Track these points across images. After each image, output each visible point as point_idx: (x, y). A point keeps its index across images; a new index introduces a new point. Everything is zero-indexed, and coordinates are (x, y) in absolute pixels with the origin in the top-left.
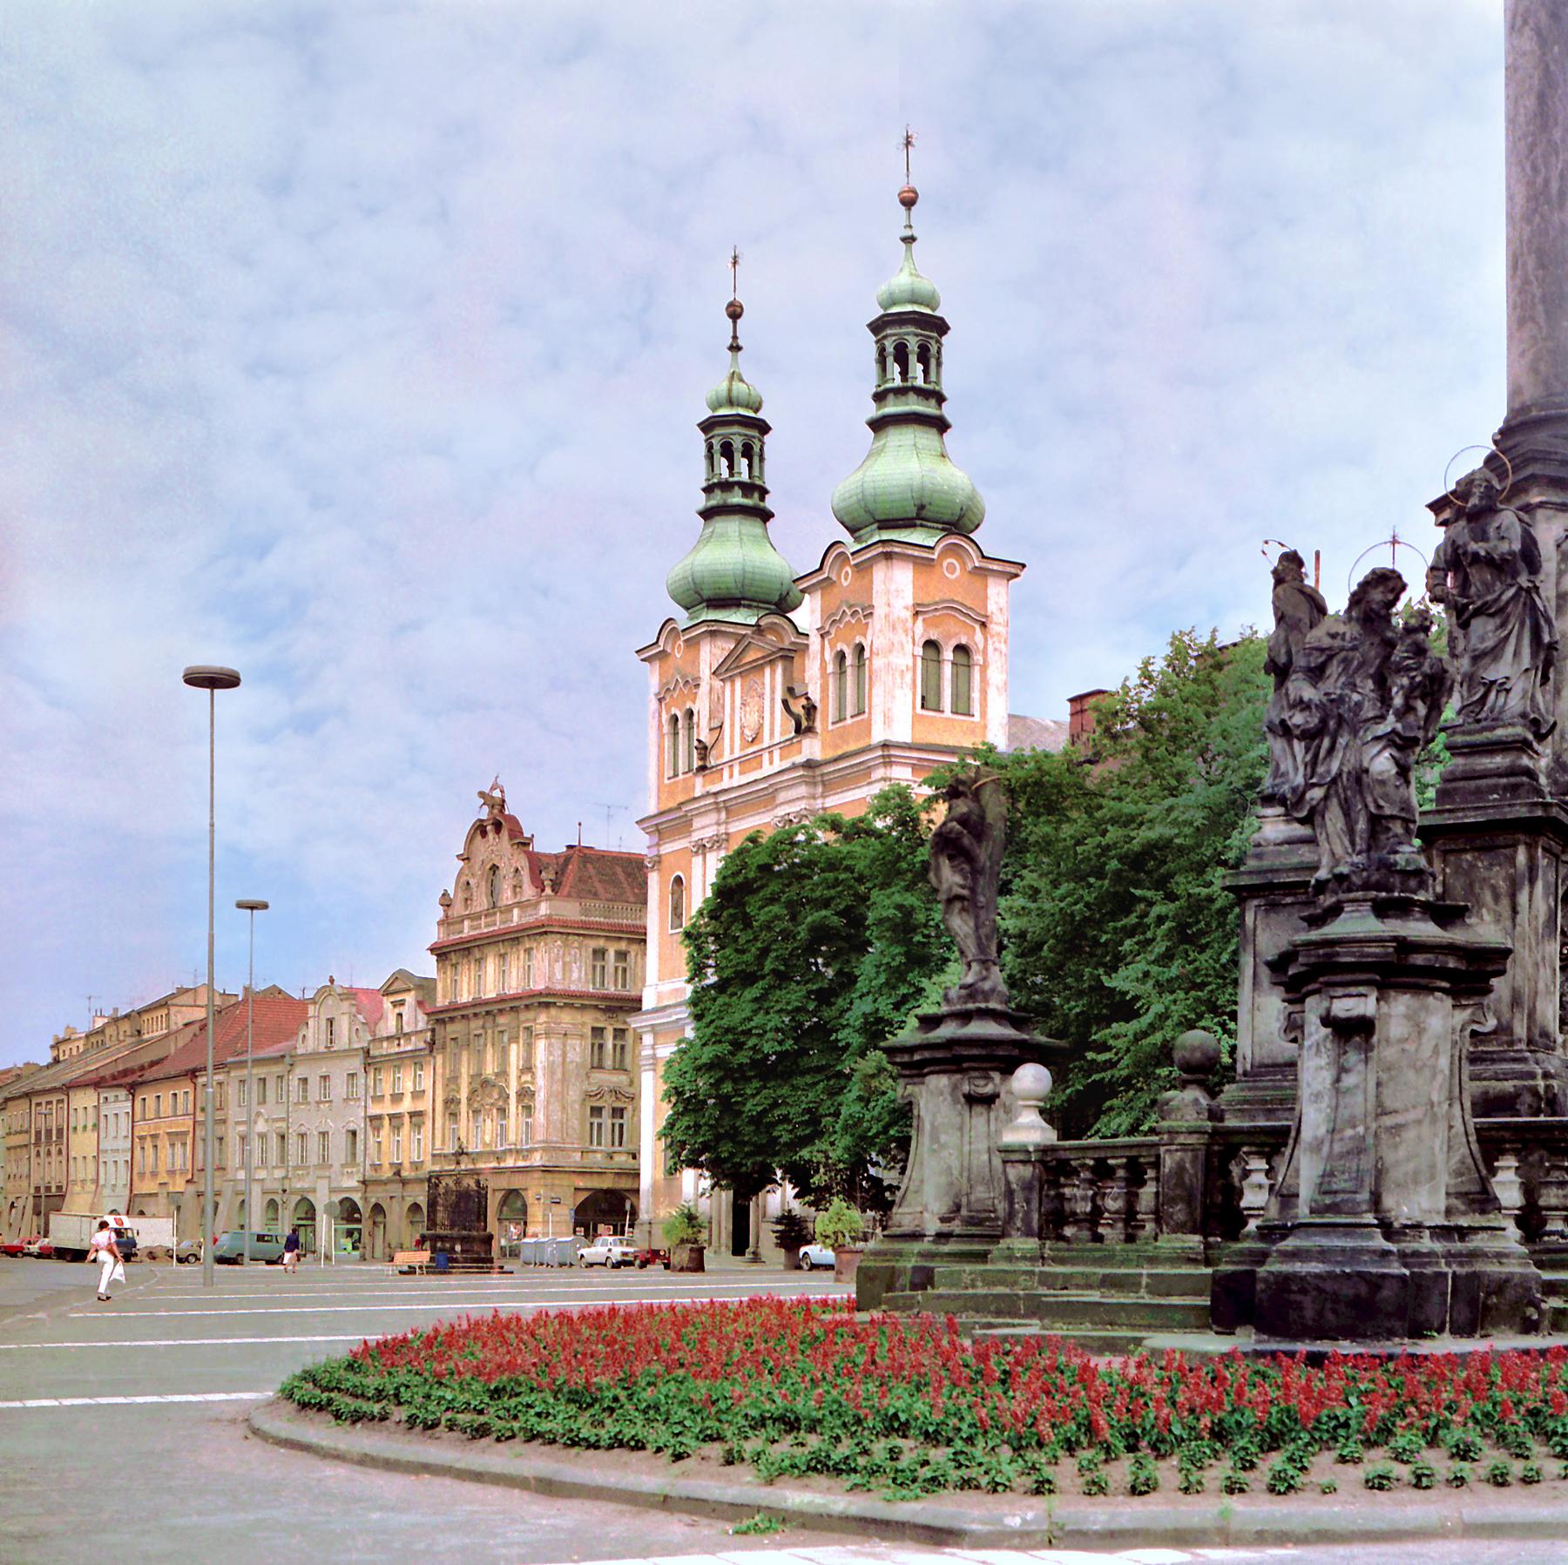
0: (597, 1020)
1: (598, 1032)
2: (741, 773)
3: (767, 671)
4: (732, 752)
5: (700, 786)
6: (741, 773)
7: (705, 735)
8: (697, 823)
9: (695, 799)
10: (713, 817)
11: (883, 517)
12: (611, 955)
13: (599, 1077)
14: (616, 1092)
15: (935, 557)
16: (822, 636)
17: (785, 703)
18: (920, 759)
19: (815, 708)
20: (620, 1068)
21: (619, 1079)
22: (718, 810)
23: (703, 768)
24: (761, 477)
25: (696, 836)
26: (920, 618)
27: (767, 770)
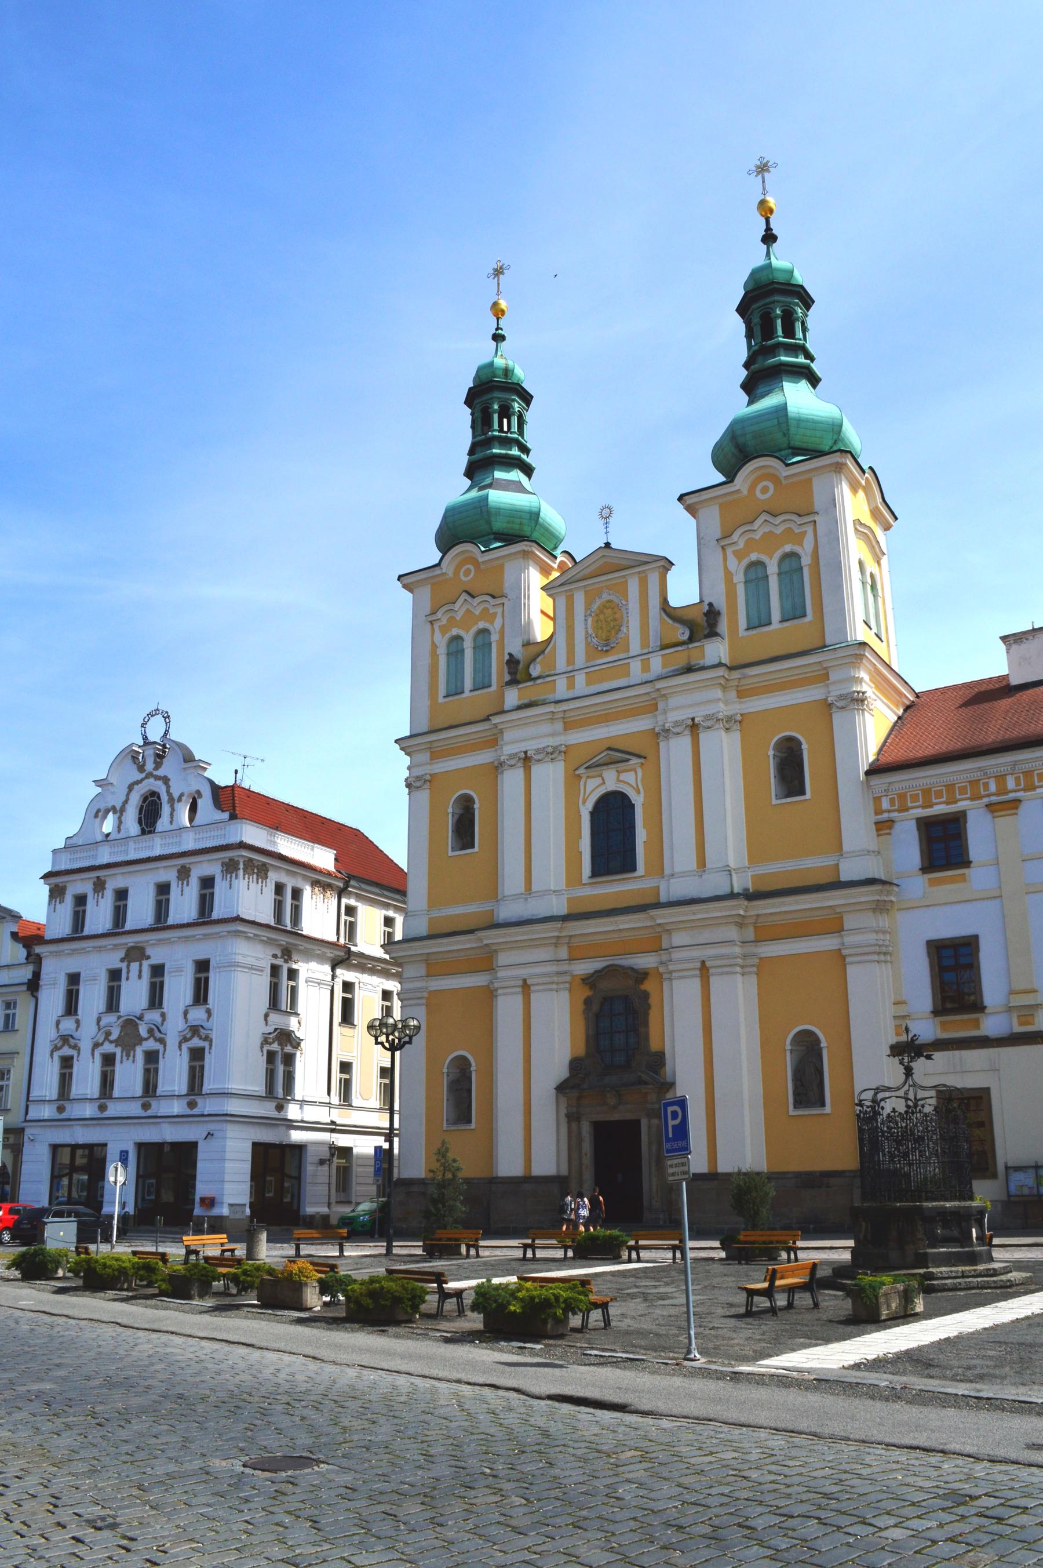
5: (512, 697)
8: (508, 736)
10: (546, 728)
17: (664, 610)
19: (719, 613)
23: (513, 682)
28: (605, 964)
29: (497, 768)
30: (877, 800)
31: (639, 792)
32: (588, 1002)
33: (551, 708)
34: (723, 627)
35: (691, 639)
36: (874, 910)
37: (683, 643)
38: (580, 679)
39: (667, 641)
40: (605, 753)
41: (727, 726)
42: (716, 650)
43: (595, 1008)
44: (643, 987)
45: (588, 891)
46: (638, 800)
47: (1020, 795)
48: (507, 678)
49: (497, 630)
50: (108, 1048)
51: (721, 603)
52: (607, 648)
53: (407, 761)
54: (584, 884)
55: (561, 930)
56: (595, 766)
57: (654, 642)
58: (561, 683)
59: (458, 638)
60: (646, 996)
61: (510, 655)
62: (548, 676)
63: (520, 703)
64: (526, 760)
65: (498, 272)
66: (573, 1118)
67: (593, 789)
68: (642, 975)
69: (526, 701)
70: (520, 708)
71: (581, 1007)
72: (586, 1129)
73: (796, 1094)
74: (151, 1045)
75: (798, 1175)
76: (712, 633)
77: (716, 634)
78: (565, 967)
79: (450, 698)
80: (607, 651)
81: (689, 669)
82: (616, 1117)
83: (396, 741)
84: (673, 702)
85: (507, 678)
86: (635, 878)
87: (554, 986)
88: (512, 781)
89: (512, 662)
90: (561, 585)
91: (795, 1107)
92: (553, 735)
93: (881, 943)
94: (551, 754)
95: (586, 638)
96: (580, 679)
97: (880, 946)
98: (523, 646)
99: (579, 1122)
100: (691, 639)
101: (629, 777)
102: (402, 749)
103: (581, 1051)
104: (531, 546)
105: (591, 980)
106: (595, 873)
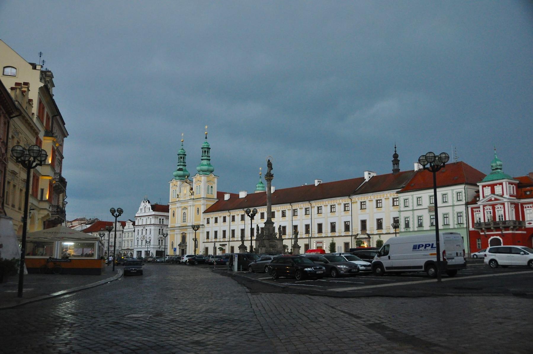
1: (160, 230)
4: (182, 196)
9: (177, 201)
10: (179, 204)
12: (161, 220)
25: (177, 206)
33: (179, 202)
34: (194, 194)
42: (192, 197)
45: (183, 224)
46: (186, 213)
50: (142, 239)
56: (183, 209)
58: (181, 199)
60: (186, 236)
66: (180, 249)
68: (186, 234)
72: (181, 250)
74: (146, 239)
76: (193, 195)
88: (177, 209)
89: (178, 195)
94: (180, 207)
103: (181, 242)
106: (183, 222)
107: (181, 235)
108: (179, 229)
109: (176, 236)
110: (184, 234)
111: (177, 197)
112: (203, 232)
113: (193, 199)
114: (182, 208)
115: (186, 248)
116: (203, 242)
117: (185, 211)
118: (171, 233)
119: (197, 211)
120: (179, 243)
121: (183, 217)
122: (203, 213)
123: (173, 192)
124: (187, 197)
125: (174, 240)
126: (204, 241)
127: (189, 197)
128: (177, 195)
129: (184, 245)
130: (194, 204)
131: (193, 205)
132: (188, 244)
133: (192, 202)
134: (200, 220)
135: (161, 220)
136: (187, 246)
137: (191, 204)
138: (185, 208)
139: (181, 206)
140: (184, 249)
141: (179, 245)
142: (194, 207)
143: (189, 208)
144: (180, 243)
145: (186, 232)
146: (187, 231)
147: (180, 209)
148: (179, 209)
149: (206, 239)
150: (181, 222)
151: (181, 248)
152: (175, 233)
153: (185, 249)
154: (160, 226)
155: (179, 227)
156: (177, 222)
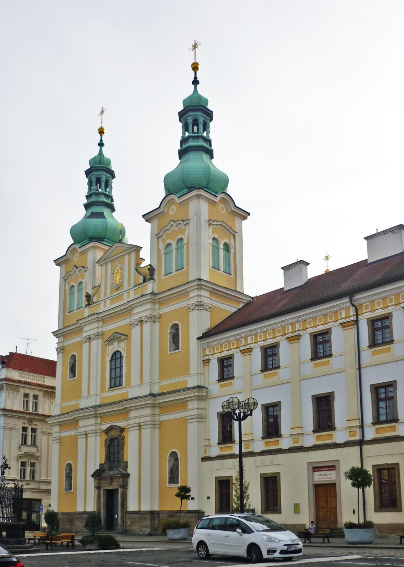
0: (24, 423)
1: (24, 429)
2: (111, 304)
3: (126, 258)
4: (105, 295)
5: (87, 312)
6: (111, 304)
7: (90, 292)
8: (85, 329)
10: (95, 325)
11: (190, 186)
12: (31, 397)
13: (25, 449)
14: (32, 456)
15: (217, 201)
16: (158, 238)
17: (136, 269)
18: (214, 289)
19: (154, 269)
20: (34, 444)
21: (32, 450)
22: (98, 321)
24: (111, 193)
25: (85, 335)
26: (211, 227)
27: (125, 299)
28: (109, 425)
29: (80, 344)
30: (204, 350)
31: (124, 351)
32: (106, 441)
35: (144, 281)
36: (198, 399)
37: (142, 284)
38: (108, 302)
39: (136, 284)
40: (114, 335)
41: (154, 320)
42: (150, 287)
43: (108, 443)
44: (123, 434)
46: (124, 354)
47: (252, 346)
48: (87, 303)
49: (85, 282)
51: (155, 266)
52: (117, 288)
53: (56, 340)
54: (107, 391)
55: (96, 411)
56: (110, 341)
57: (132, 284)
58: (102, 304)
59: (73, 286)
61: (87, 293)
62: (99, 301)
63: (90, 314)
64: (89, 339)
65: (195, 46)
66: (98, 488)
67: (111, 350)
68: (122, 430)
69: (91, 313)
70: (89, 316)
71: (104, 443)
72: (102, 491)
73: (170, 478)
75: (169, 512)
77: (154, 279)
78: (99, 427)
79: (70, 313)
80: (117, 289)
81: (143, 296)
82: (111, 488)
83: (52, 333)
84: (136, 311)
85: (87, 303)
86: (123, 388)
87: (94, 434)
88: (86, 346)
89: (88, 297)
90: (103, 261)
91: (169, 484)
92: (98, 328)
93: (200, 413)
94: (98, 336)
95: (111, 284)
96: (108, 302)
97: (199, 415)
98: (93, 288)
99: (100, 489)
100: (144, 281)
101: (122, 344)
102: (54, 336)
104: (95, 244)
105: (106, 431)
106: (111, 387)
107: (105, 437)
108: (96, 416)
109: (81, 442)
110: (113, 434)
111: (84, 302)
112: (201, 418)
113: (153, 293)
114: (107, 336)
115: (125, 486)
116: (205, 459)
117: (121, 347)
118: (63, 434)
119: (168, 338)
120: (94, 467)
121: (111, 370)
122: (199, 338)
123: (71, 294)
124: (125, 294)
125: (76, 461)
126: (207, 455)
127: (132, 292)
128: (84, 298)
129: (116, 472)
130: (156, 313)
131: (154, 319)
132: (132, 470)
133: (149, 306)
134: (185, 369)
135: (31, 397)
136: (128, 475)
137: (143, 315)
138: (117, 336)
139: (100, 330)
140: (117, 490)
141: (97, 475)
142: (157, 324)
143: (135, 332)
144: (101, 465)
145: (122, 424)
146: (127, 419)
147: (97, 344)
148: (94, 343)
149: (219, 444)
150: (103, 389)
151: (106, 486)
152: (80, 430)
153: (120, 490)
154: (27, 416)
155: (96, 407)
156: (84, 393)
